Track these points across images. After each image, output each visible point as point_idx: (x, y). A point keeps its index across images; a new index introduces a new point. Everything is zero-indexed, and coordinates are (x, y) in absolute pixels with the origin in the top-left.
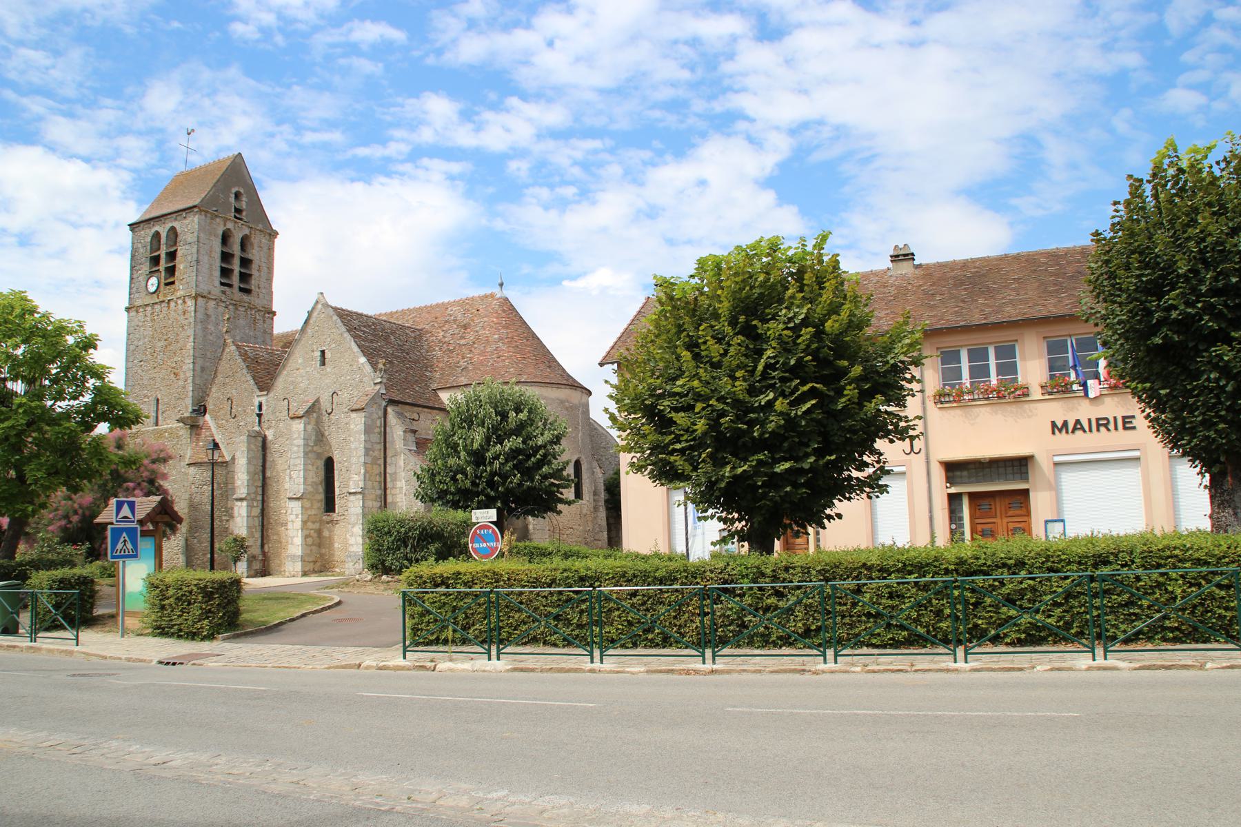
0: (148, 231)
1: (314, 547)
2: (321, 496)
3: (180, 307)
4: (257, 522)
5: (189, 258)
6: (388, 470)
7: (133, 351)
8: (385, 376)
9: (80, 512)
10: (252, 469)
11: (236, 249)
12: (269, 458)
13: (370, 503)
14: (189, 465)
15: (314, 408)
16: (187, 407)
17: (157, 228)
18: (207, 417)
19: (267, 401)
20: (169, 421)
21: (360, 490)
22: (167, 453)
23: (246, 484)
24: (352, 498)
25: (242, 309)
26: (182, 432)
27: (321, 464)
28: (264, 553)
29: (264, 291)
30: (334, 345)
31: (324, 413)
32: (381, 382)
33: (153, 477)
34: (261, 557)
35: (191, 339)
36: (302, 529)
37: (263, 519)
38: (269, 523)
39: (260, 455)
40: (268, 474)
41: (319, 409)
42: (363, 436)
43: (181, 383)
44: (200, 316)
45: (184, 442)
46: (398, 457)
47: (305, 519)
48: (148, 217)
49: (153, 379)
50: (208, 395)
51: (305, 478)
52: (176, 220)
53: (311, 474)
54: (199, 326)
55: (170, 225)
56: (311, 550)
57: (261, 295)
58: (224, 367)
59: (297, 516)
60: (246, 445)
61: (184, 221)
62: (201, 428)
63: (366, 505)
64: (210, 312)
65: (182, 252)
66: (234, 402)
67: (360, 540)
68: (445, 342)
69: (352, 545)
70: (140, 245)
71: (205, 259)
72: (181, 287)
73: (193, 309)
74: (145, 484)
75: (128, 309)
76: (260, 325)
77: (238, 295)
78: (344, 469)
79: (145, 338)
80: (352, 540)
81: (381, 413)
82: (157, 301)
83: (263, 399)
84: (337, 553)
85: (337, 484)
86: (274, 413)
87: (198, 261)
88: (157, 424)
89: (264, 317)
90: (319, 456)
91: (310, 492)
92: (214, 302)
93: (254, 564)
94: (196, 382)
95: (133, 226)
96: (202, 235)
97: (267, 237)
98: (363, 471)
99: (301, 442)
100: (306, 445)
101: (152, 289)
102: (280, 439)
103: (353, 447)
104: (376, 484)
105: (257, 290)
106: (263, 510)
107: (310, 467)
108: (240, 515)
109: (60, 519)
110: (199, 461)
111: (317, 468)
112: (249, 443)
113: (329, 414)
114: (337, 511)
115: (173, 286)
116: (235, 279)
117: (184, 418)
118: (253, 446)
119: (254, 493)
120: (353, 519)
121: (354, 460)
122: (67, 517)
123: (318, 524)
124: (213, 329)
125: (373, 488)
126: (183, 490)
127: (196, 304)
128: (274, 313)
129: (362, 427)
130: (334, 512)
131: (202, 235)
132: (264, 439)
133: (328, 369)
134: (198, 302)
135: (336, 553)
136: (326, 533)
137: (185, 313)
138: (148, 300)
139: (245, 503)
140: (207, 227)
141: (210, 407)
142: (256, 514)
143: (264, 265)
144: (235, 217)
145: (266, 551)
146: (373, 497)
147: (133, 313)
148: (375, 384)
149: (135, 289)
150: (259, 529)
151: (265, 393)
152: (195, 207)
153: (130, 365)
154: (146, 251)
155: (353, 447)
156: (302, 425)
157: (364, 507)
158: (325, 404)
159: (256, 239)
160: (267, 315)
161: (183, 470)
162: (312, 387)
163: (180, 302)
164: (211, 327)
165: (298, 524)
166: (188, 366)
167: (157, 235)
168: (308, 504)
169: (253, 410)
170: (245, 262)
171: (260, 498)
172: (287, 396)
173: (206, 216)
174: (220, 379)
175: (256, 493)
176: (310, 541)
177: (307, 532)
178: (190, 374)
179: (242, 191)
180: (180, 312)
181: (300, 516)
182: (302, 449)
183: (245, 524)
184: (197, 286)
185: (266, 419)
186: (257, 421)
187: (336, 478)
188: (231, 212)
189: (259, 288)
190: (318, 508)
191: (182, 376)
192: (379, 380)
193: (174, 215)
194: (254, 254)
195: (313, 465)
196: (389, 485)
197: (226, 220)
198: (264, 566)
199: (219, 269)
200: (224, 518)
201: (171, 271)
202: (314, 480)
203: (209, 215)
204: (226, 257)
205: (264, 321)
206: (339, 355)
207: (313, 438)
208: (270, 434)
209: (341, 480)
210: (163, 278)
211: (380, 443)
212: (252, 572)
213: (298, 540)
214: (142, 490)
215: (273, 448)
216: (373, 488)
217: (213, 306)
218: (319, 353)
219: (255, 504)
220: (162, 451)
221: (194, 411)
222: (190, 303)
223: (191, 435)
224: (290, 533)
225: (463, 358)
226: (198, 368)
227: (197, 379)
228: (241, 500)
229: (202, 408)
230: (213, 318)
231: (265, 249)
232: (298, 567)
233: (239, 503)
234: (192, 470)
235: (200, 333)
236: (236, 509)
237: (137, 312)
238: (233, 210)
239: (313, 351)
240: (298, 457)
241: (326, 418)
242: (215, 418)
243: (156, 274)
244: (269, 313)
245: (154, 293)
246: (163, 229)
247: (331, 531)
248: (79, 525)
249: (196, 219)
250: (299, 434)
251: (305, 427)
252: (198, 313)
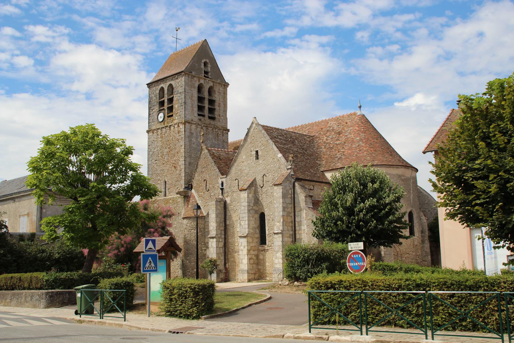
0: (157, 87)
1: (254, 265)
2: (258, 235)
3: (176, 129)
4: (222, 250)
5: (180, 101)
6: (297, 220)
7: (152, 155)
8: (293, 164)
9: (125, 245)
10: (218, 220)
11: (206, 95)
12: (228, 214)
13: (286, 239)
14: (184, 218)
15: (253, 184)
16: (181, 185)
17: (162, 85)
18: (193, 191)
19: (226, 181)
20: (172, 194)
21: (280, 231)
22: (172, 212)
23: (215, 229)
24: (276, 236)
25: (210, 129)
26: (179, 200)
27: (257, 216)
28: (226, 268)
29: (222, 118)
30: (263, 147)
31: (259, 187)
32: (291, 168)
33: (164, 225)
34: (224, 271)
35: (183, 147)
36: (248, 255)
37: (225, 249)
38: (229, 251)
39: (223, 212)
40: (228, 223)
41: (256, 185)
42: (281, 200)
43: (178, 172)
44: (188, 134)
45: (181, 205)
46: (302, 212)
47: (249, 248)
48: (157, 79)
49: (163, 170)
50: (193, 179)
51: (249, 225)
52: (172, 80)
53: (252, 222)
54: (187, 140)
55: (169, 83)
56: (253, 267)
57: (221, 120)
58: (201, 162)
59: (244, 247)
60: (215, 206)
62: (190, 198)
63: (284, 240)
64: (193, 131)
65: (176, 98)
66: (208, 182)
67: (281, 261)
68: (328, 143)
69: (276, 264)
70: (153, 95)
71: (189, 101)
73: (183, 130)
74: (160, 229)
75: (148, 132)
76: (220, 137)
77: (208, 121)
78: (271, 219)
79: (157, 147)
80: (276, 261)
81: (291, 186)
82: (164, 126)
83: (224, 180)
84: (268, 268)
85: (267, 228)
86: (230, 187)
87: (185, 103)
88: (165, 196)
89: (223, 133)
90: (256, 212)
91: (252, 233)
92: (195, 126)
93: (220, 275)
94: (187, 171)
95: (149, 85)
96: (187, 88)
97: (223, 87)
98: (282, 220)
99: (246, 204)
100: (249, 206)
101: (161, 120)
102: (234, 203)
103: (276, 206)
104: (290, 228)
105: (219, 117)
106: (225, 243)
107: (251, 218)
108: (212, 246)
109: (114, 250)
110: (189, 216)
111: (255, 219)
112: (216, 205)
113: (262, 187)
114: (267, 244)
115: (172, 118)
116: (206, 112)
117: (180, 192)
118: (219, 207)
119: (220, 234)
120: (277, 248)
121: (276, 214)
122: (118, 248)
123: (257, 252)
124: (195, 140)
125: (288, 230)
126: (180, 233)
127: (185, 127)
128: (228, 130)
129: (280, 194)
130: (265, 244)
131: (187, 88)
132: (225, 202)
133: (260, 161)
134: (186, 126)
135: (267, 268)
136: (261, 257)
138: (159, 126)
139: (215, 240)
140: (189, 83)
141: (194, 185)
142: (221, 246)
143: (222, 103)
144: (205, 76)
145: (227, 267)
146: (288, 235)
147: (151, 134)
148: (288, 169)
149: (151, 120)
150: (223, 254)
151: (225, 176)
152: (182, 72)
153: (150, 163)
155: (276, 206)
156: (246, 195)
157: (283, 241)
158: (259, 182)
159: (217, 89)
160: (224, 132)
161: (180, 221)
162: (251, 172)
163: (176, 126)
164: (194, 140)
165: (245, 252)
166: (182, 162)
167: (162, 89)
168: (250, 240)
169: (219, 186)
170: (212, 102)
171: (223, 236)
172: (238, 178)
173: (188, 77)
174: (199, 169)
175: (221, 234)
176: (252, 261)
177: (250, 256)
178: (183, 167)
179: (208, 61)
180: (176, 132)
181: (246, 247)
182: (246, 208)
183: (215, 252)
184: (185, 117)
185: (226, 191)
186: (221, 192)
187: (266, 225)
188: (202, 74)
189: (219, 116)
190: (257, 242)
191: (179, 168)
192: (290, 167)
193: (171, 77)
194: (216, 97)
195: (253, 217)
196: (297, 228)
197: (199, 79)
198: (226, 276)
199: (197, 106)
200: (203, 248)
201: (171, 109)
202: (254, 226)
203: (190, 76)
204: (200, 99)
205: (223, 135)
206: (266, 153)
207: (253, 201)
208: (228, 200)
209: (269, 226)
210: (166, 113)
211: (291, 204)
212: (220, 280)
213: (245, 261)
214: (158, 233)
215: (230, 207)
216: (288, 230)
217: (195, 128)
218: (255, 152)
219: (221, 240)
220: (169, 211)
221: (186, 187)
222: (182, 126)
223: (184, 201)
224: (241, 257)
225: (339, 152)
226: (187, 163)
227: (187, 169)
228: (213, 238)
229: (190, 186)
230: (195, 135)
231: (222, 94)
232: (246, 277)
233: (211, 240)
234: (185, 221)
235: (187, 143)
236: (210, 243)
237: (153, 133)
238: (203, 73)
239: (251, 151)
240: (245, 213)
241: (259, 190)
242: (197, 191)
244: (225, 130)
245: (162, 122)
246: (165, 86)
247: (264, 256)
248: (125, 253)
249: (183, 79)
250: (245, 199)
251: (248, 195)
252: (186, 132)
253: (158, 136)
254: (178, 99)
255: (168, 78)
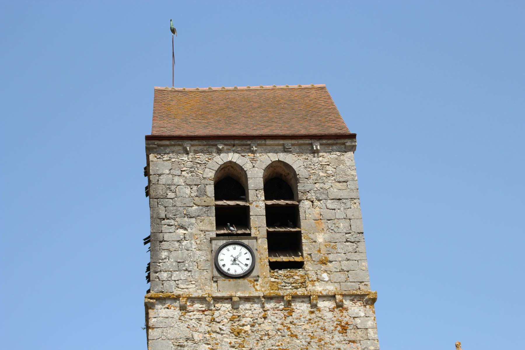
0: (202, 157)
52: (286, 150)
55: (274, 157)
61: (315, 160)
72: (325, 276)
115: (301, 272)
137: (344, 329)
138: (213, 289)
154: (202, 193)
193: (288, 143)
237: (183, 308)
243: (246, 242)
245: (244, 276)
253: (216, 327)
254: (329, 214)
255: (269, 142)
